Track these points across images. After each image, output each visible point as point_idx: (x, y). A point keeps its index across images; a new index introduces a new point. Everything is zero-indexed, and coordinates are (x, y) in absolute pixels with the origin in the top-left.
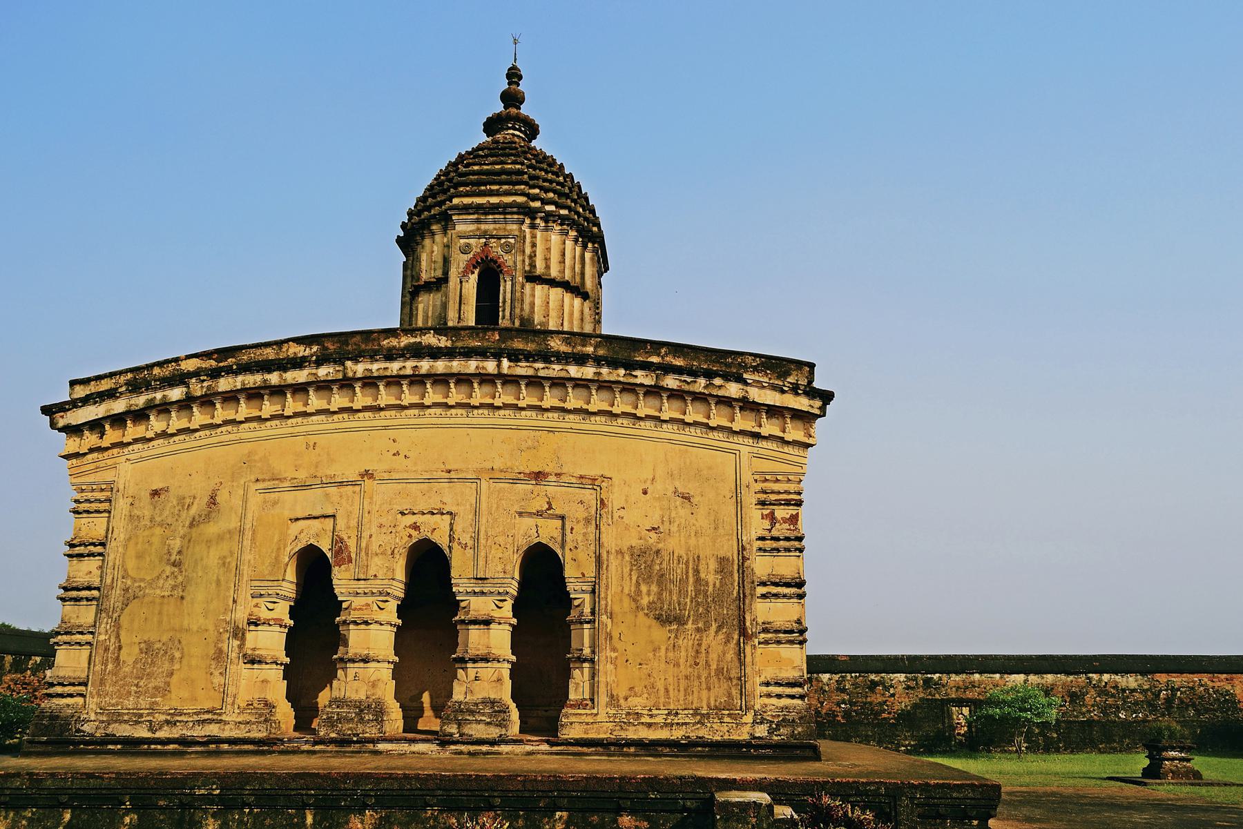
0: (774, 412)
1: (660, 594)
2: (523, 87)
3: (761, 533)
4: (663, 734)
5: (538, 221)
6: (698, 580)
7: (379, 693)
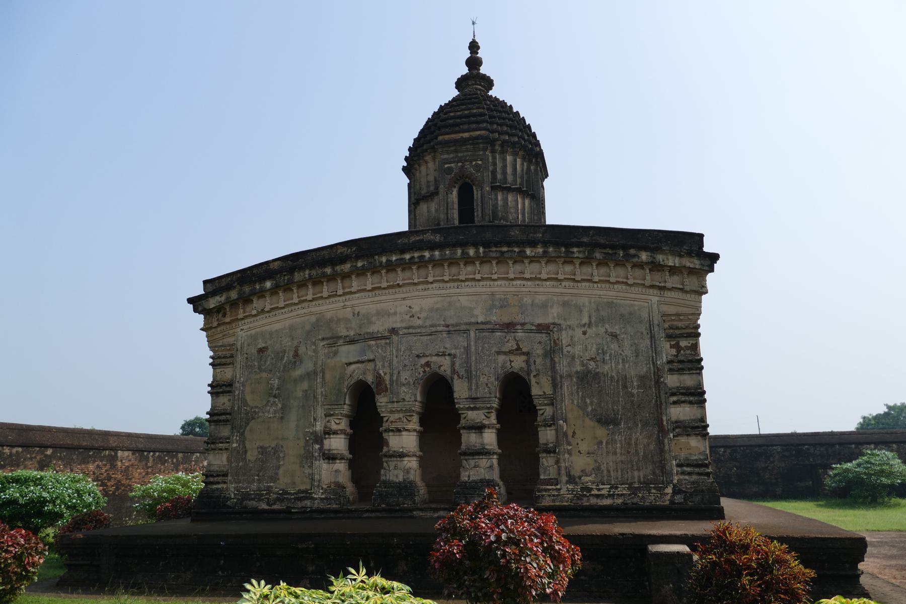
0: (673, 270)
4: (608, 502)
5: (497, 147)
7: (412, 477)
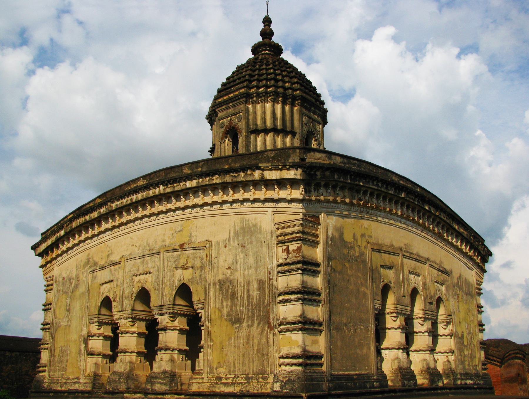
1: (231, 306)
2: (272, 26)
3: (281, 261)
6: (249, 296)
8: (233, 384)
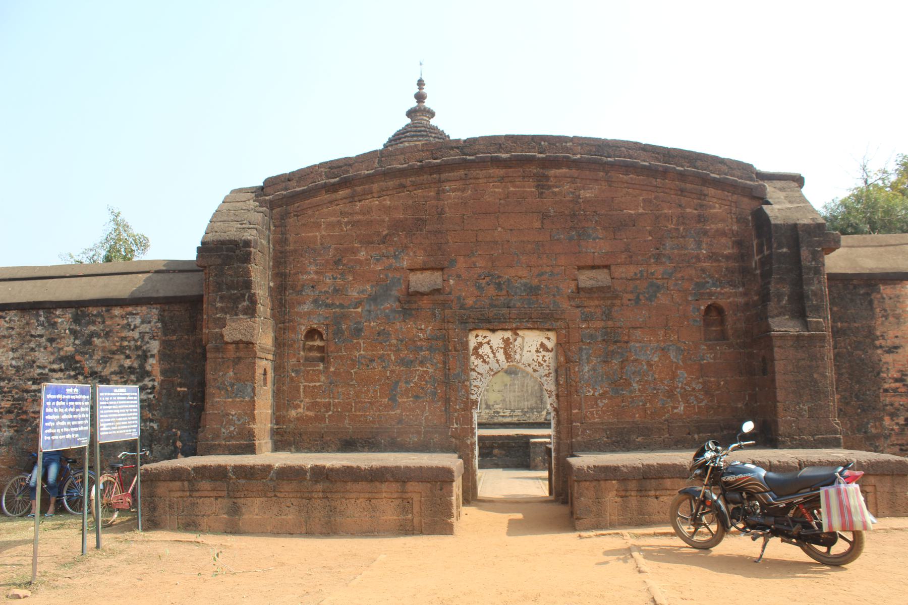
8: (511, 416)
